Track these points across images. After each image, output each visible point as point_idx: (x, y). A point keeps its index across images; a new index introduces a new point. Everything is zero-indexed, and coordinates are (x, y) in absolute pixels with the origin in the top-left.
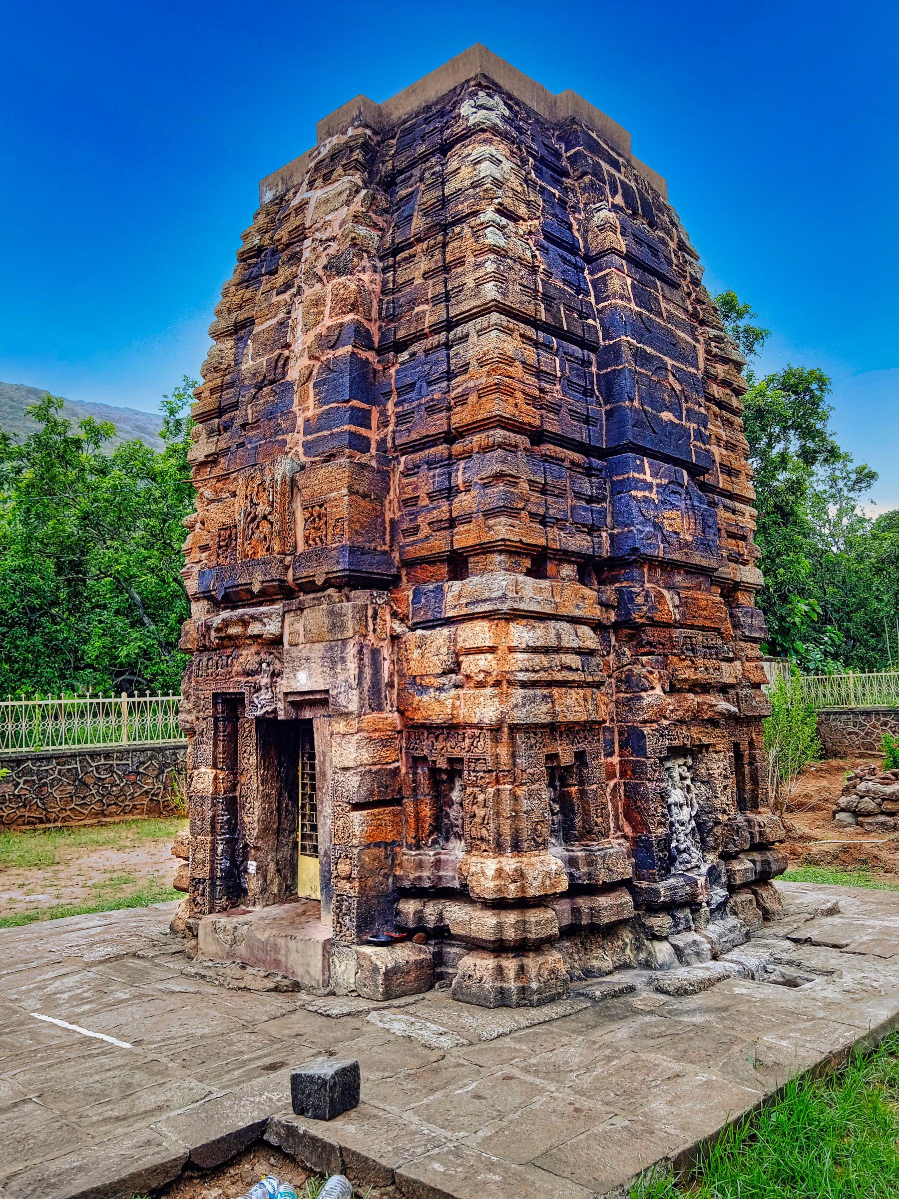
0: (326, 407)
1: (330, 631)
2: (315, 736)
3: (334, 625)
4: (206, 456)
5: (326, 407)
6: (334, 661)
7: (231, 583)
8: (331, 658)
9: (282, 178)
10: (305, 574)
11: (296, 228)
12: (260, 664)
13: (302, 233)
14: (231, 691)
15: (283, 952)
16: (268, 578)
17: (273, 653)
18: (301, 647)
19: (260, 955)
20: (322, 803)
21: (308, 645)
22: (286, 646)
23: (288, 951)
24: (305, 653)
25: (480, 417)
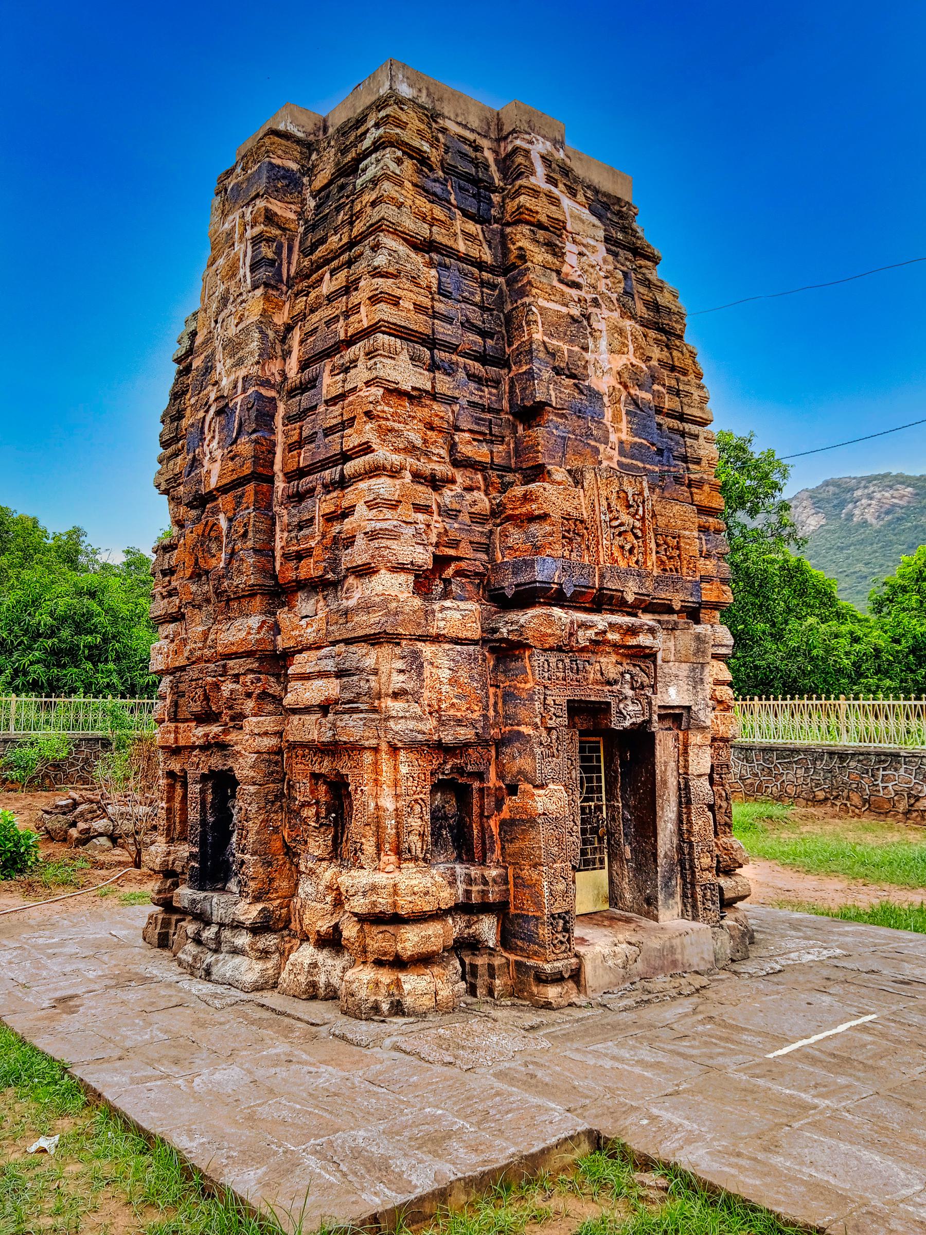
0: (637, 439)
1: (694, 655)
2: (658, 747)
3: (698, 650)
4: (414, 388)
5: (637, 439)
6: (697, 682)
7: (582, 581)
8: (694, 678)
9: (427, 89)
10: (664, 596)
11: (557, 219)
12: (622, 674)
13: (559, 230)
14: (593, 699)
15: (679, 951)
16: (644, 591)
17: (639, 666)
18: (671, 664)
19: (657, 963)
20: (662, 810)
21: (677, 664)
22: (659, 662)
23: (683, 947)
24: (674, 671)
25: (714, 506)
